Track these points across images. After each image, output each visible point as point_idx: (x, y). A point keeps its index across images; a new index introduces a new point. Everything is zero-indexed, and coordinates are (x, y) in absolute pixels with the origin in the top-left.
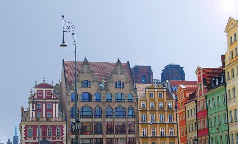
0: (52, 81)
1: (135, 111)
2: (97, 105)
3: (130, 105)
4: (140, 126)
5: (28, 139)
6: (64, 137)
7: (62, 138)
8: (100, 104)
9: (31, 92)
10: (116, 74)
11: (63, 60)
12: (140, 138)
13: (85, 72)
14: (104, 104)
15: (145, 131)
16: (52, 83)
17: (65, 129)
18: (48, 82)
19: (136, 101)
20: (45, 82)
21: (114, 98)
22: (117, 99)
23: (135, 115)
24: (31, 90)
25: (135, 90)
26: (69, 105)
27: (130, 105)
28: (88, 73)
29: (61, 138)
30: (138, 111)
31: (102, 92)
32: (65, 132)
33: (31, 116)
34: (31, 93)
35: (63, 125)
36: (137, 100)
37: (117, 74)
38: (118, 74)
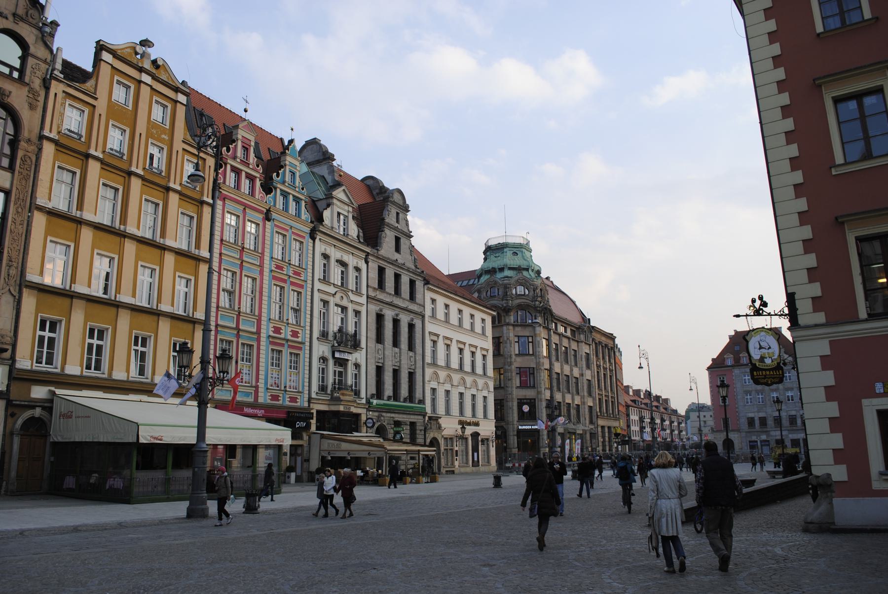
1: (25, 133)
12: (25, 292)
19: (37, 83)
23: (20, 154)
30: (42, 137)
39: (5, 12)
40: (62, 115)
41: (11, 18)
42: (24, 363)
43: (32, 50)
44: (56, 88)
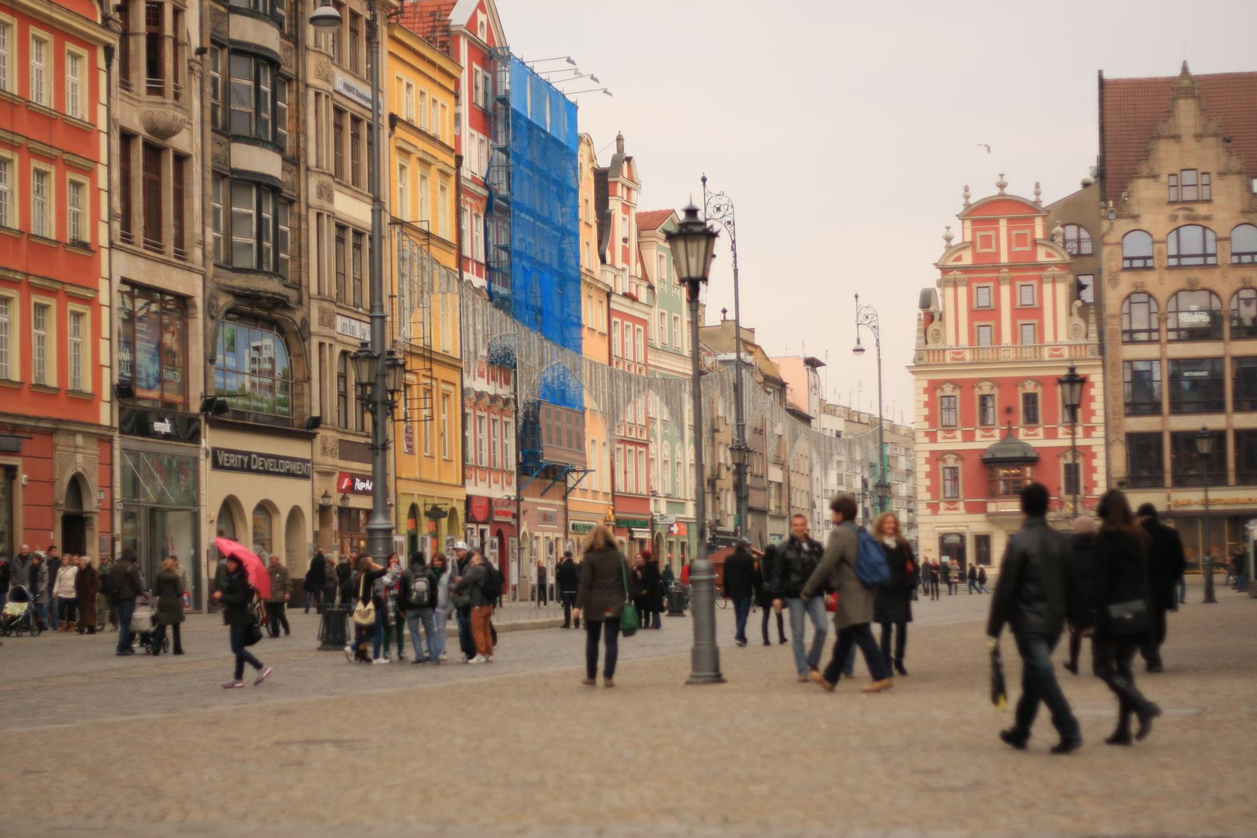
0: (1037, 186)
5: (939, 439)
6: (1093, 428)
7: (1088, 431)
9: (948, 239)
13: (1183, 131)
16: (1038, 194)
17: (1097, 391)
18: (1020, 189)
24: (948, 228)
28: (1199, 137)
32: (1098, 406)
34: (944, 243)
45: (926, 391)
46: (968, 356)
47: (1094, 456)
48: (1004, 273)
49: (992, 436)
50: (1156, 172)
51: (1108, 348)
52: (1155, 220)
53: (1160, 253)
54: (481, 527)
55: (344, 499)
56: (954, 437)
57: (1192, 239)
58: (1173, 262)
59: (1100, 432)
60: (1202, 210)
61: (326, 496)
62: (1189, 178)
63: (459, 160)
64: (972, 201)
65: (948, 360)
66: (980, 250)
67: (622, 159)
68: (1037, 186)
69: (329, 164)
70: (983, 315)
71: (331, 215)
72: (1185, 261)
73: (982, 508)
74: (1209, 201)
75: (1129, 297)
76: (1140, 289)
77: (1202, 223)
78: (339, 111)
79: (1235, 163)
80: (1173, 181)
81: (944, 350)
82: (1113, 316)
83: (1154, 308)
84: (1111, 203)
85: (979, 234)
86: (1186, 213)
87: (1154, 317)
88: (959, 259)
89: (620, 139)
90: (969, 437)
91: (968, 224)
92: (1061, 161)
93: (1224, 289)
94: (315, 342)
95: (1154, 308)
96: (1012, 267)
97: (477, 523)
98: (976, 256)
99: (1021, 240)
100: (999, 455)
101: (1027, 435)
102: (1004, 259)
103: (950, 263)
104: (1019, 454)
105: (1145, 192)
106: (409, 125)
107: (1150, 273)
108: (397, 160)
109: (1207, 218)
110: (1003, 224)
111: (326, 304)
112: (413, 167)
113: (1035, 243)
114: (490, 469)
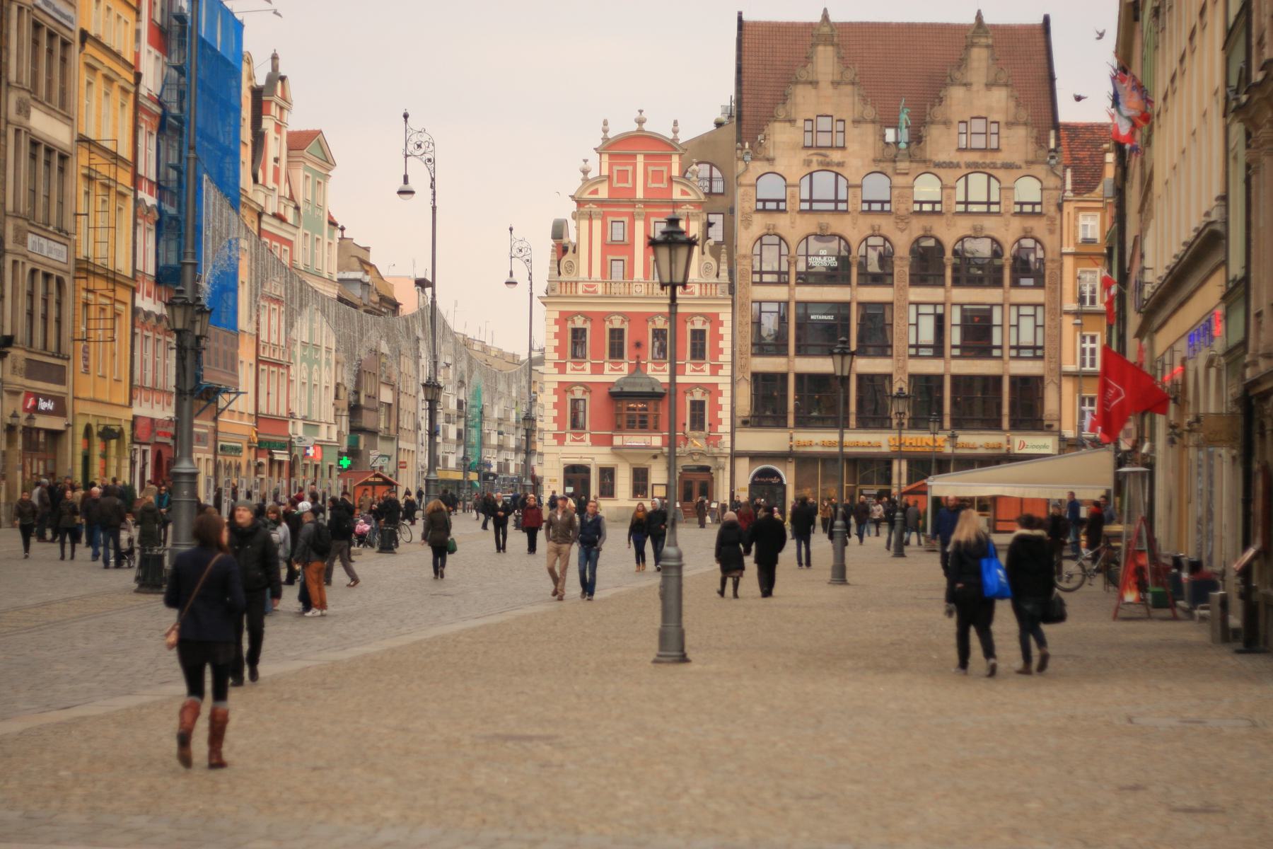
0: (676, 123)
2: (873, 228)
3: (1025, 230)
4: (1068, 322)
5: (568, 371)
6: (721, 367)
7: (715, 370)
8: (886, 225)
9: (585, 172)
10: (965, 85)
11: (740, 14)
13: (820, 78)
14: (902, 225)
15: (1093, 346)
16: (675, 132)
17: (726, 330)
18: (659, 126)
19: (1052, 210)
20: (646, 127)
21: (949, 198)
22: (967, 203)
24: (585, 161)
25: (1052, 157)
26: (747, 228)
27: (1025, 230)
28: (836, 84)
29: (707, 367)
30: (1062, 254)
31: (895, 169)
32: (726, 344)
33: (584, 274)
34: (582, 175)
35: (717, 315)
36: (1060, 207)
37: (971, 84)
38: (975, 88)
39: (1018, 163)
40: (1076, 227)
41: (1024, 166)
42: (1069, 433)
43: (1045, 183)
44: (1069, 208)
45: (557, 322)
46: (600, 289)
47: (720, 393)
48: (639, 208)
49: (621, 370)
50: (793, 116)
51: (738, 287)
52: (791, 164)
53: (793, 196)
54: (144, 447)
55: (30, 418)
56: (583, 370)
57: (824, 185)
58: (806, 206)
59: (727, 370)
60: (836, 156)
61: (14, 415)
62: (824, 124)
63: (138, 77)
64: (610, 135)
65: (580, 292)
66: (615, 184)
67: (276, 78)
68: (676, 123)
69: (26, 80)
70: (616, 249)
71: (28, 131)
72: (816, 206)
73: (608, 441)
74: (843, 148)
75: (760, 238)
76: (771, 232)
77: (835, 169)
78: (37, 26)
79: (870, 112)
80: (808, 126)
81: (576, 283)
82: (745, 257)
83: (784, 250)
84: (747, 145)
85: (616, 168)
86: (820, 158)
87: (784, 259)
88: (595, 192)
89: (275, 58)
90: (597, 369)
91: (605, 158)
92: (696, 98)
93: (854, 237)
94: (9, 259)
95: (784, 250)
96: (646, 203)
97: (141, 444)
98: (612, 189)
99: (657, 176)
100: (626, 389)
101: (655, 370)
102: (640, 194)
103: (586, 196)
104: (648, 389)
105: (781, 136)
106: (97, 41)
107: (783, 216)
108: (85, 76)
109: (840, 164)
110: (640, 159)
111: (20, 222)
112: (99, 83)
113: (671, 179)
114: (153, 389)
